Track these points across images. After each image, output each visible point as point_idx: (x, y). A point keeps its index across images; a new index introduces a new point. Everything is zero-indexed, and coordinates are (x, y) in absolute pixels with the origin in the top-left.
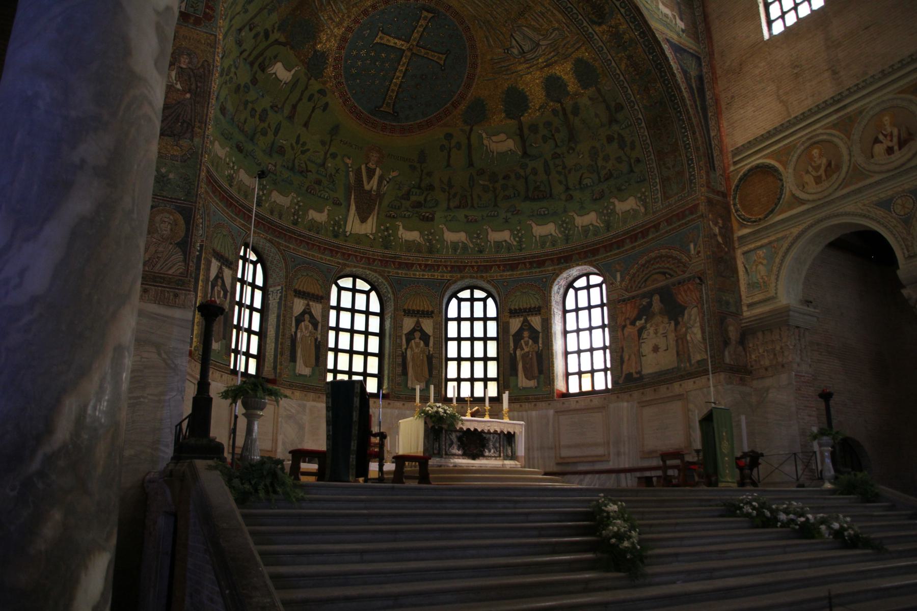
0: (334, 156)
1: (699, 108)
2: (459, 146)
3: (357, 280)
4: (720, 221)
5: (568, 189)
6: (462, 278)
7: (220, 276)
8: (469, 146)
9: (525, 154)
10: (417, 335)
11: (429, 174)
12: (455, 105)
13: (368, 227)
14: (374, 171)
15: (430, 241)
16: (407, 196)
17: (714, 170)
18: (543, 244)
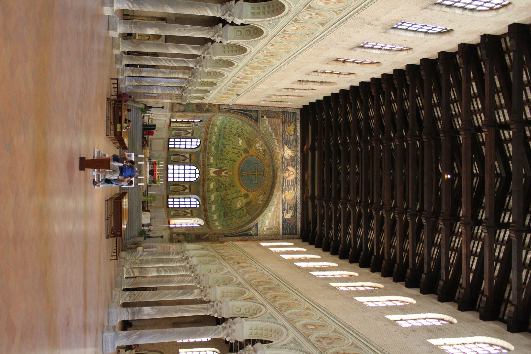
0: (228, 162)
1: (242, 233)
2: (238, 195)
3: (199, 174)
4: (210, 237)
5: (226, 220)
6: (201, 199)
7: (189, 133)
8: (238, 197)
9: (236, 210)
10: (184, 188)
11: (229, 189)
12: (247, 191)
13: (212, 174)
14: (227, 174)
15: (211, 191)
16: (223, 184)
17: (225, 237)
18: (211, 217)
